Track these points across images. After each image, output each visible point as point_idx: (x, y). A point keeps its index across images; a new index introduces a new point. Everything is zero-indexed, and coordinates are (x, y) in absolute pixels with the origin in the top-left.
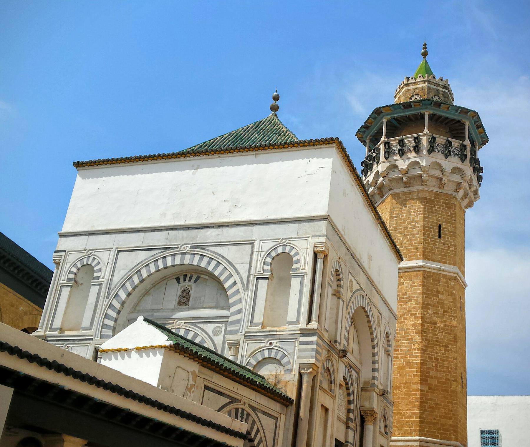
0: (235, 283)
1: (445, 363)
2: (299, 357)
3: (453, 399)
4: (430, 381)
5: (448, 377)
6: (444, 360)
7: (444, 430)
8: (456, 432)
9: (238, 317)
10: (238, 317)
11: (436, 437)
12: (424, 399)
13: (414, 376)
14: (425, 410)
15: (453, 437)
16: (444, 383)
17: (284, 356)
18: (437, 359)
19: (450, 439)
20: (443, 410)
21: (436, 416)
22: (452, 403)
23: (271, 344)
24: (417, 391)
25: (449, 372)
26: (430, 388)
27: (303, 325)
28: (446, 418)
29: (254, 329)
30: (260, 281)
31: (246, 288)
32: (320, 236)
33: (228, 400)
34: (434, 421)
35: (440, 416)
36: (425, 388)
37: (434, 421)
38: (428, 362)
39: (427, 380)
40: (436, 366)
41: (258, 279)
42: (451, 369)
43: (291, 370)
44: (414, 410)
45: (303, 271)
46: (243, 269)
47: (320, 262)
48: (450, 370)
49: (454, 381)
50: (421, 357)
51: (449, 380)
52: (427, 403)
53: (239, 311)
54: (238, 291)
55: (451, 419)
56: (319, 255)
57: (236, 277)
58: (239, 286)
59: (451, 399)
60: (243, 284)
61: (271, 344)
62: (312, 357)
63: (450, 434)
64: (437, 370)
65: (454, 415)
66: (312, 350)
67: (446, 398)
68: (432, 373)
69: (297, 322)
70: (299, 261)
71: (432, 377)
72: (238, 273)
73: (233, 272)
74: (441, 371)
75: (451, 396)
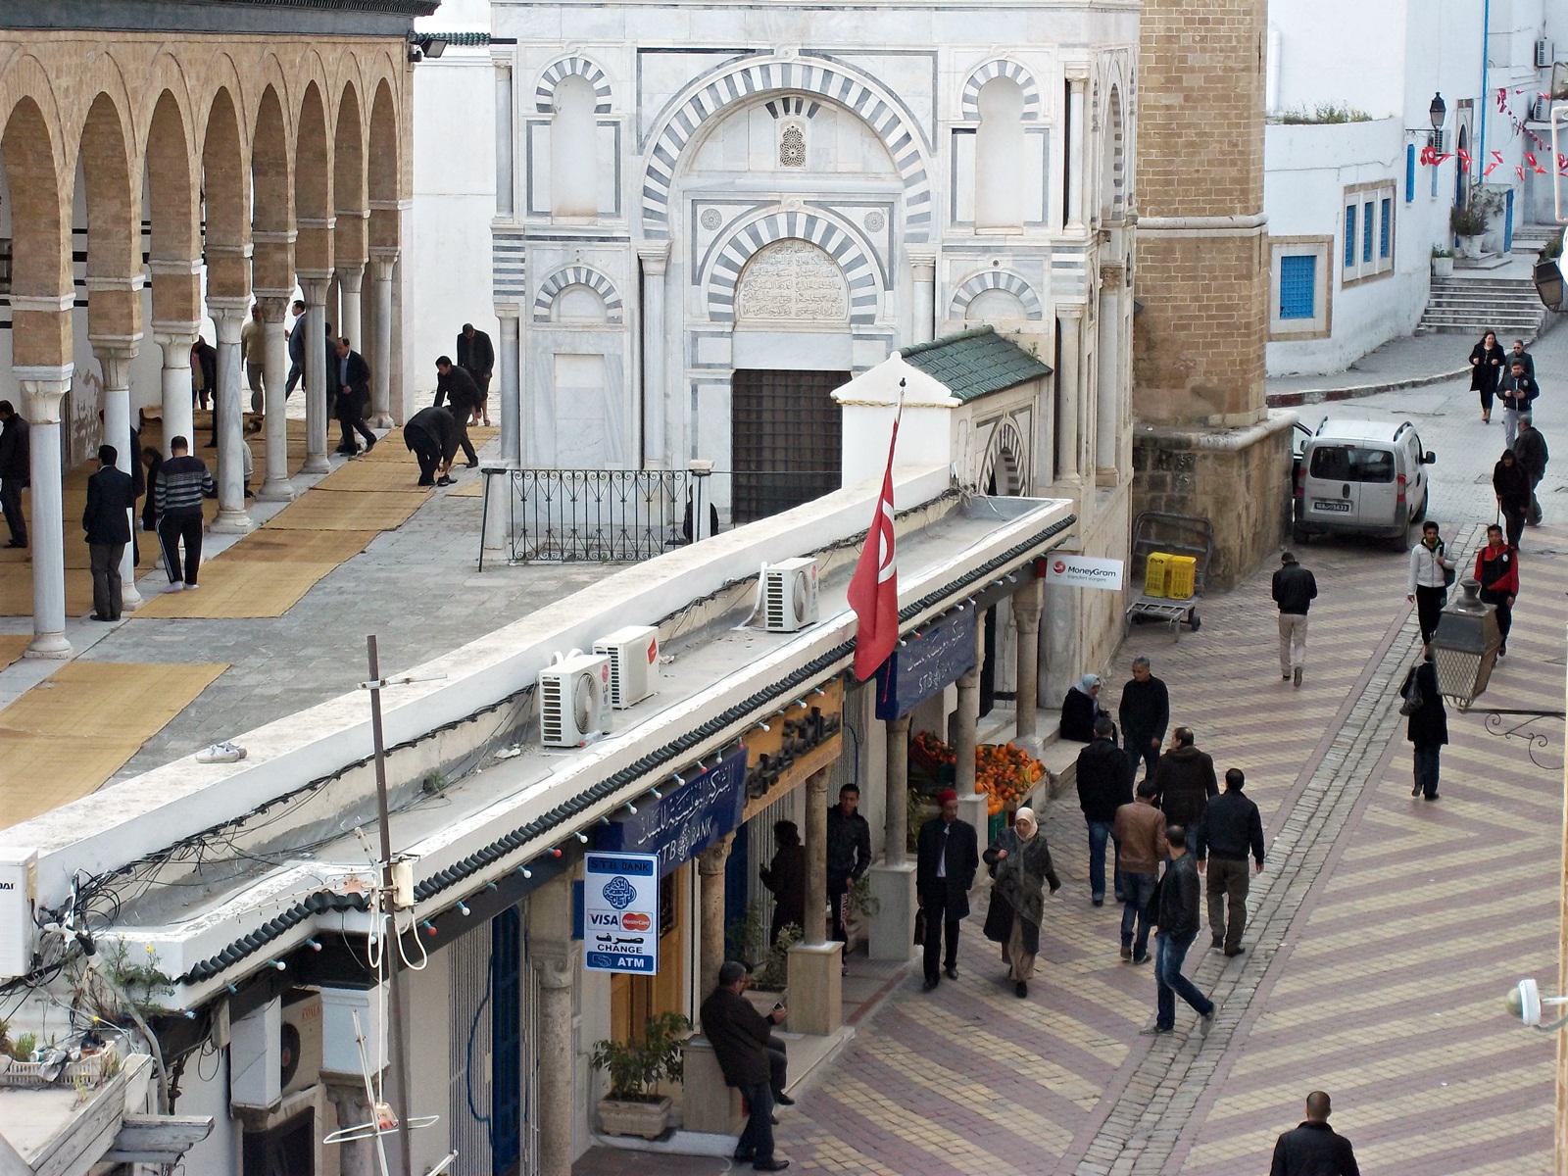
0: (908, 137)
1: (1224, 29)
2: (1053, 292)
3: (1239, 116)
4: (1188, 80)
5: (1231, 63)
6: (1221, 22)
7: (1218, 192)
8: (1245, 192)
9: (924, 207)
10: (924, 207)
11: (1200, 212)
12: (1174, 126)
13: (1151, 70)
14: (1177, 154)
15: (1238, 205)
16: (1221, 80)
17: (1024, 287)
18: (1204, 21)
19: (1230, 212)
20: (1218, 146)
21: (1201, 163)
22: (1238, 125)
23: (996, 263)
24: (1156, 108)
25: (1234, 49)
26: (1187, 98)
27: (1054, 229)
28: (1222, 163)
29: (960, 232)
30: (960, 136)
31: (933, 148)
32: (1074, 46)
33: (993, 424)
34: (1196, 176)
35: (1210, 163)
36: (1175, 99)
37: (1196, 176)
38: (1184, 31)
39: (1179, 80)
40: (1203, 39)
41: (954, 131)
42: (1239, 42)
43: (1039, 315)
44: (1150, 154)
45: (1048, 120)
46: (922, 109)
47: (1076, 99)
48: (1234, 43)
49: (1243, 70)
50: (1168, 21)
51: (1232, 69)
52: (1180, 136)
53: (925, 197)
54: (916, 155)
55: (1233, 163)
56: (1075, 87)
57: (906, 125)
58: (917, 143)
59: (1239, 116)
60: (925, 140)
61: (996, 263)
62: (1079, 293)
63: (1231, 201)
64: (1204, 50)
65: (1241, 153)
66: (1080, 279)
67: (1226, 116)
68: (1193, 60)
69: (1044, 223)
70: (1034, 98)
71: (1192, 70)
72: (912, 117)
73: (901, 113)
74: (1214, 50)
75: (1236, 108)
